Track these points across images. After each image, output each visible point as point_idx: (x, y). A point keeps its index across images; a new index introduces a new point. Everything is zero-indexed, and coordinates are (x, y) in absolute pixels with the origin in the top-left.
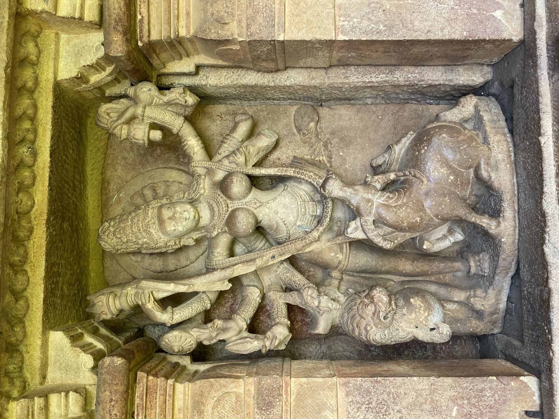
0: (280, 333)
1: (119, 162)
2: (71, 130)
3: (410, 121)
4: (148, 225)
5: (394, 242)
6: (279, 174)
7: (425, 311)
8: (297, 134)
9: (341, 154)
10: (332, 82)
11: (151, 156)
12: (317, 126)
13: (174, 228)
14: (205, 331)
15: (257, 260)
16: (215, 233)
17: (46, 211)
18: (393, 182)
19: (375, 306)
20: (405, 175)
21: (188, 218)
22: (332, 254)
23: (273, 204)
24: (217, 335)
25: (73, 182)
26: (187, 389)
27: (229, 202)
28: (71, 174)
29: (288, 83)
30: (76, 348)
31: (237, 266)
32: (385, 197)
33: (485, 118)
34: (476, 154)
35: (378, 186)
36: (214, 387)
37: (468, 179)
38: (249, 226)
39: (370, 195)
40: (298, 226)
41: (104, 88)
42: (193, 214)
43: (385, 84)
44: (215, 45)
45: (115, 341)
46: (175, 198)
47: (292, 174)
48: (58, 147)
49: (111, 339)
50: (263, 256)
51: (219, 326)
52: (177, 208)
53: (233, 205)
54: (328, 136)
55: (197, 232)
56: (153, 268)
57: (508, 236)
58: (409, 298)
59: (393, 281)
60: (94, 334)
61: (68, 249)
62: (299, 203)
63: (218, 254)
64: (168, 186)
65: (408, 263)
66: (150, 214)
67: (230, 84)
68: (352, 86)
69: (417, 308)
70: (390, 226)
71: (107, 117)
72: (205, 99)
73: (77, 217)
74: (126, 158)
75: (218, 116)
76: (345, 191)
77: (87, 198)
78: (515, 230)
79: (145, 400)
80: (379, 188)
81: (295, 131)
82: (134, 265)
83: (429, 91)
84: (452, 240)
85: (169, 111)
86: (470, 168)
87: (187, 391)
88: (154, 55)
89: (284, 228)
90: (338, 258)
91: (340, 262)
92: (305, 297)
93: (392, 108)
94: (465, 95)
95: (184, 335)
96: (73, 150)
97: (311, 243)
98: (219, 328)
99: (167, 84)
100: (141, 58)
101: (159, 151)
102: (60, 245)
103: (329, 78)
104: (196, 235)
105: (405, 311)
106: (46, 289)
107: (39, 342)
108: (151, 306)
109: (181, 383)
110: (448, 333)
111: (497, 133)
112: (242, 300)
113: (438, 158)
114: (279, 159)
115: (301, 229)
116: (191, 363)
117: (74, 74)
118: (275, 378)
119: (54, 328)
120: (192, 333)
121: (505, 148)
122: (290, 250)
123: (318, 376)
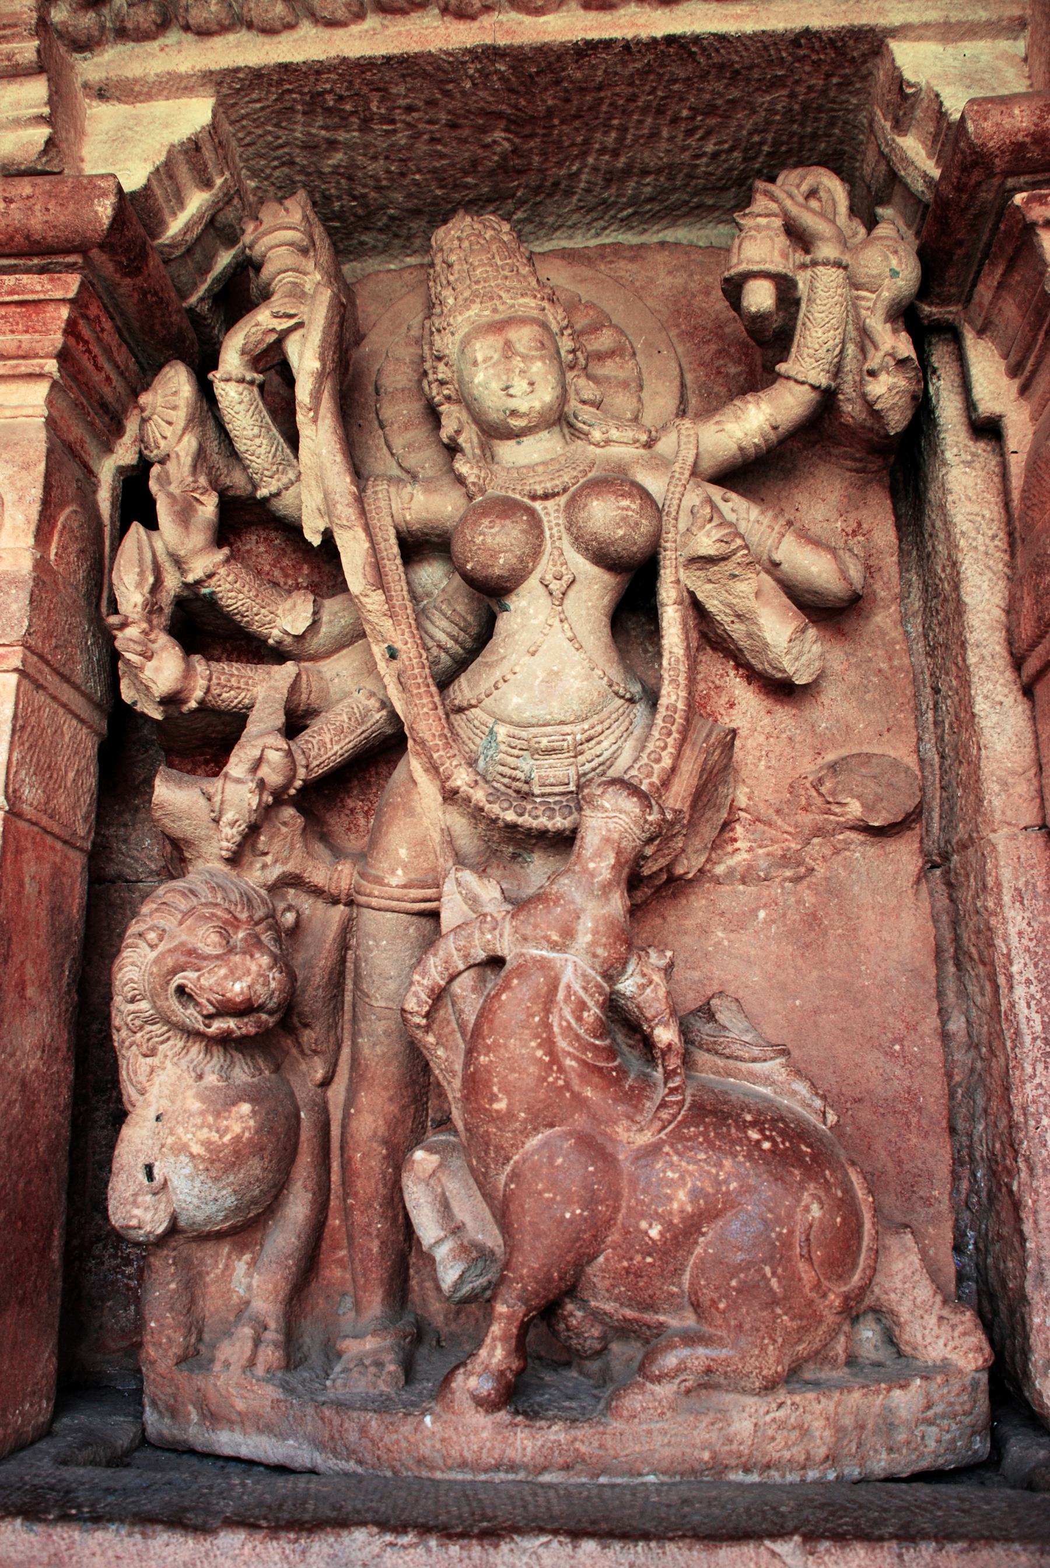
0: (160, 671)
1: (696, 277)
2: (769, 137)
3: (890, 1154)
4: (492, 298)
5: (427, 1029)
6: (665, 662)
7: (207, 1144)
8: (820, 761)
9: (762, 914)
10: (1000, 848)
11: (719, 352)
12: (852, 828)
13: (480, 358)
14: (186, 470)
15: (378, 597)
17: (517, 41)
18: (647, 1043)
19: (217, 957)
20: (669, 1075)
21: (511, 391)
22: (403, 853)
23: (558, 638)
24: (170, 495)
25: (627, 172)
26: (30, 412)
27: (563, 500)
28: (647, 157)
29: (981, 706)
30: (165, 153)
31: (362, 535)
32: (581, 993)
33: (897, 1393)
34: (747, 1326)
35: (627, 985)
36: (24, 473)
37: (650, 1306)
38: (483, 557)
39: (589, 938)
40: (491, 731)
41: (897, 199)
42: (523, 406)
43: (1008, 1034)
45: (195, 286)
46: (582, 382)
47: (663, 701)
48: (704, 76)
49: (204, 270)
50: (396, 624)
51: (200, 508)
52: (539, 364)
53: (551, 513)
54: (821, 871)
55: (475, 440)
56: (389, 368)
57: (443, 1440)
58: (253, 1101)
59: (326, 1082)
60: (212, 222)
61: (442, 156)
62: (567, 729)
63: (407, 498)
64: (625, 385)
65: (381, 1122)
66: (522, 301)
67: (957, 530)
68: (993, 921)
69: (218, 1115)
70: (485, 1014)
71: (805, 188)
72: (901, 463)
73: (537, 190)
74: (707, 294)
75: (860, 525)
76: (598, 854)
77: (598, 235)
78: (463, 1465)
79: (8, 299)
80: (620, 987)
81: (830, 757)
82: (400, 326)
83: (1003, 1215)
84: (442, 1253)
85: (843, 342)
86: (696, 1306)
87: (25, 412)
88: (1000, 271)
89: (486, 685)
90: (393, 872)
91: (379, 881)
92: (260, 743)
93: (933, 1092)
94: (988, 1324)
95: (180, 416)
96: (715, 156)
97: (433, 769)
98: (191, 505)
99: (933, 359)
100: (985, 238)
101: (733, 370)
102: (443, 117)
103: (1013, 837)
105: (211, 1079)
107: (184, 68)
108: (263, 320)
109: (50, 402)
110: (134, 1222)
111: (840, 1431)
112: (276, 584)
113: (726, 1182)
114: (732, 705)
115: (484, 743)
116: (121, 470)
117: (908, 75)
118: (20, 622)
119: (222, 107)
120: (186, 438)
121: (774, 1450)
122: (423, 720)
123: (16, 755)
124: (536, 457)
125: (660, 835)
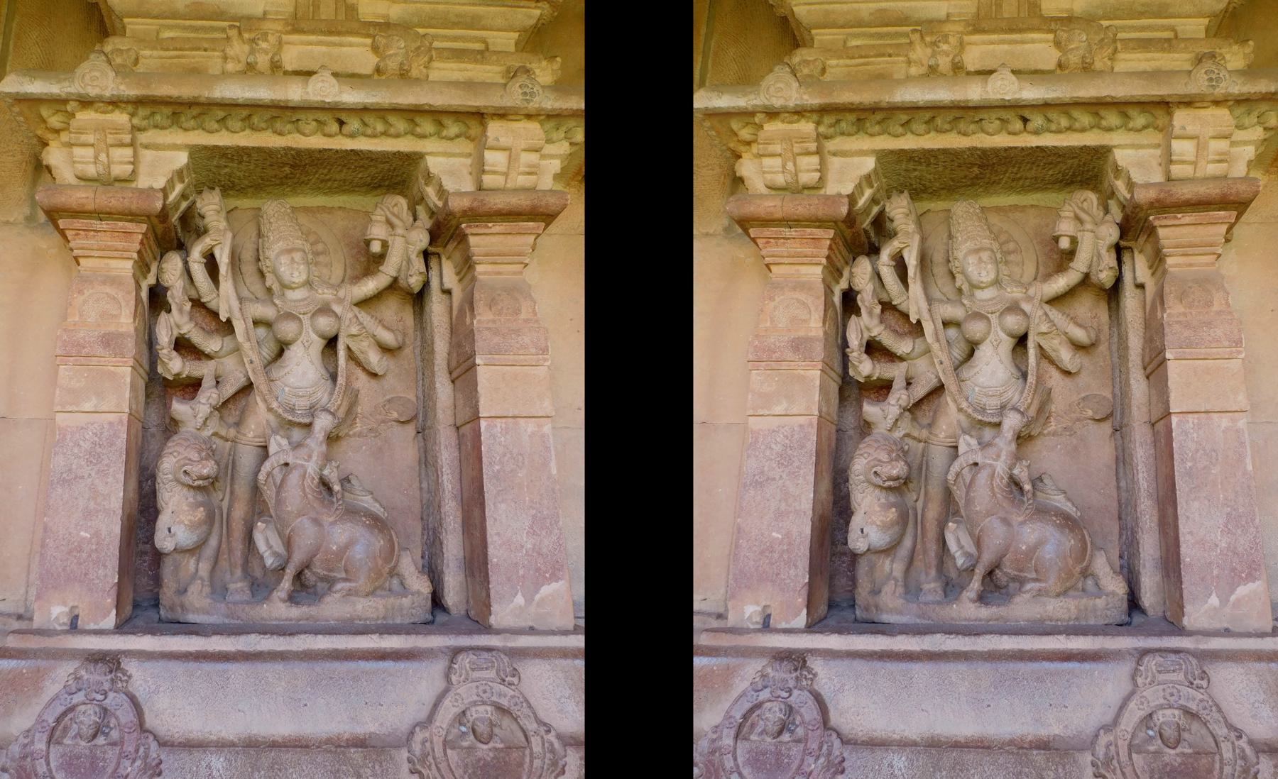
16: (277, 302)
35: (326, 472)
44: (470, 302)
78: (276, 619)
86: (346, 571)
104: (276, 287)
106: (227, 148)
107: (179, 142)
124: (299, 297)
125: (337, 427)
